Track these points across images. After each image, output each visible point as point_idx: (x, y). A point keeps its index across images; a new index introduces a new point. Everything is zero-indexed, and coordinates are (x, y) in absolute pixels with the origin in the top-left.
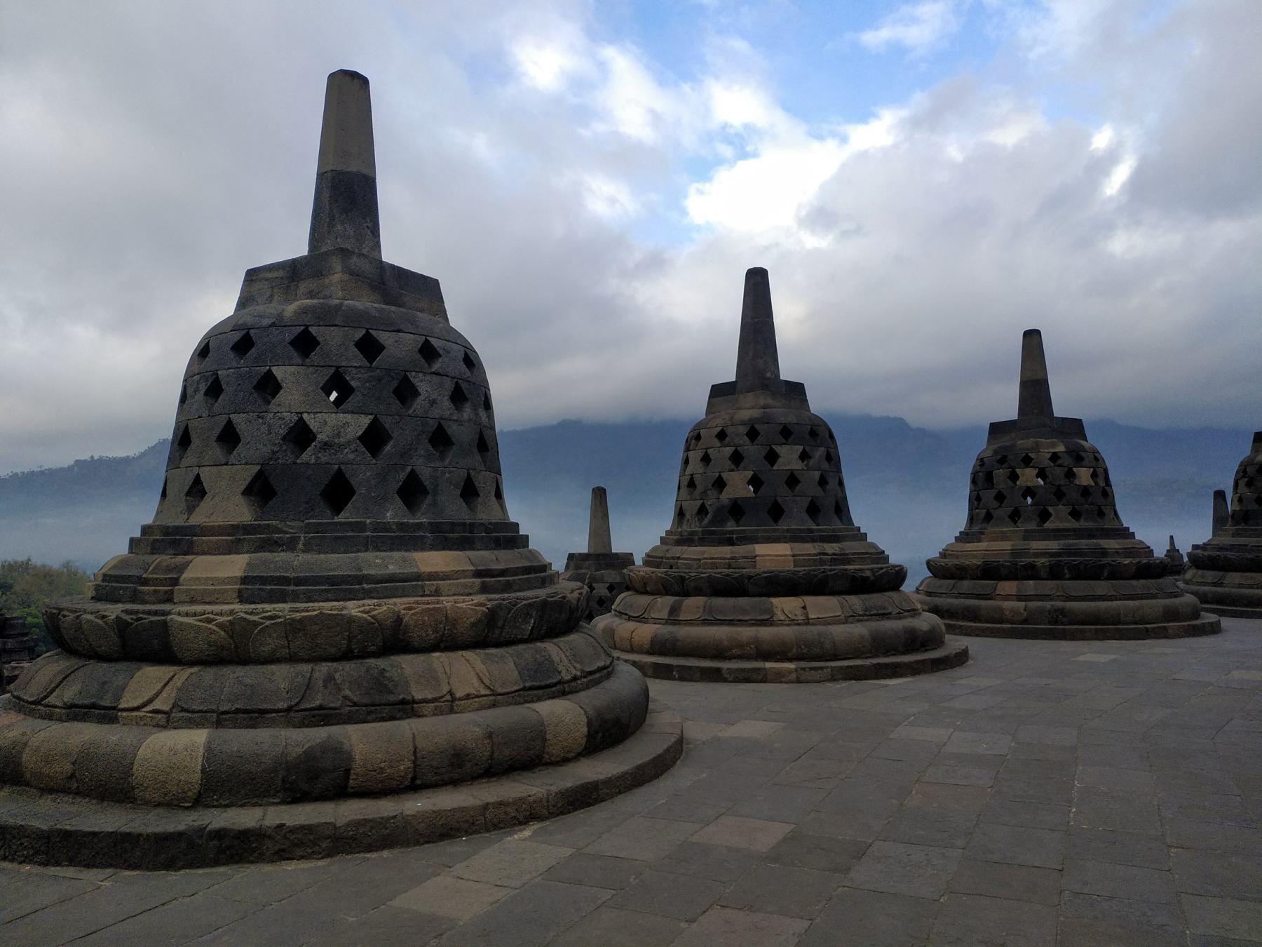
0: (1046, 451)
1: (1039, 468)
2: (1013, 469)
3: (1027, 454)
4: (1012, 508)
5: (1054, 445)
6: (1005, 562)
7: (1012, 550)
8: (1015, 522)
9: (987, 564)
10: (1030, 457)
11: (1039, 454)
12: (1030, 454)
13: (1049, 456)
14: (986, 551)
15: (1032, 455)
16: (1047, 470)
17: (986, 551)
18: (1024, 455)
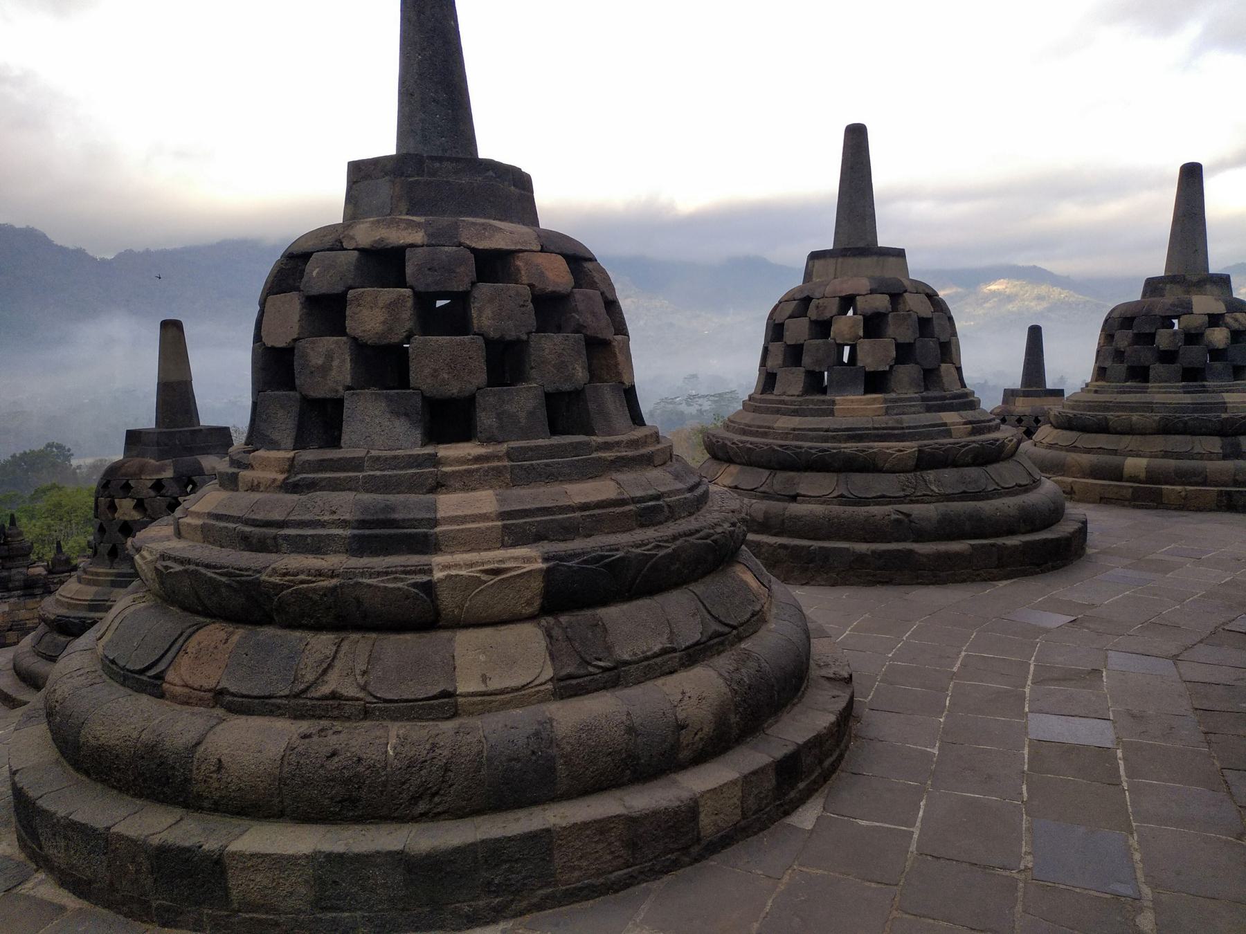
0: (148, 478)
1: (138, 500)
2: (113, 497)
3: (128, 480)
4: (111, 545)
5: (161, 469)
6: (74, 618)
7: (92, 600)
8: (112, 562)
9: (60, 620)
10: (130, 485)
11: (140, 480)
12: (130, 482)
13: (150, 484)
14: (71, 598)
15: (132, 483)
16: (146, 501)
17: (71, 598)
18: (124, 481)
